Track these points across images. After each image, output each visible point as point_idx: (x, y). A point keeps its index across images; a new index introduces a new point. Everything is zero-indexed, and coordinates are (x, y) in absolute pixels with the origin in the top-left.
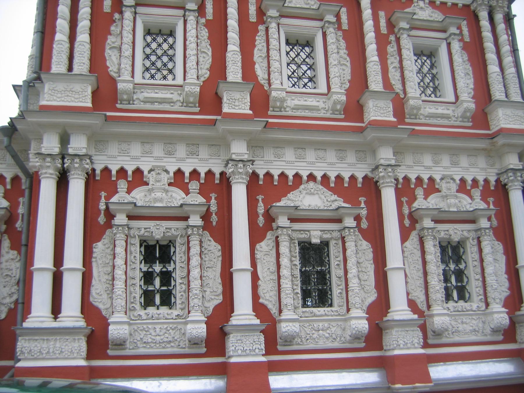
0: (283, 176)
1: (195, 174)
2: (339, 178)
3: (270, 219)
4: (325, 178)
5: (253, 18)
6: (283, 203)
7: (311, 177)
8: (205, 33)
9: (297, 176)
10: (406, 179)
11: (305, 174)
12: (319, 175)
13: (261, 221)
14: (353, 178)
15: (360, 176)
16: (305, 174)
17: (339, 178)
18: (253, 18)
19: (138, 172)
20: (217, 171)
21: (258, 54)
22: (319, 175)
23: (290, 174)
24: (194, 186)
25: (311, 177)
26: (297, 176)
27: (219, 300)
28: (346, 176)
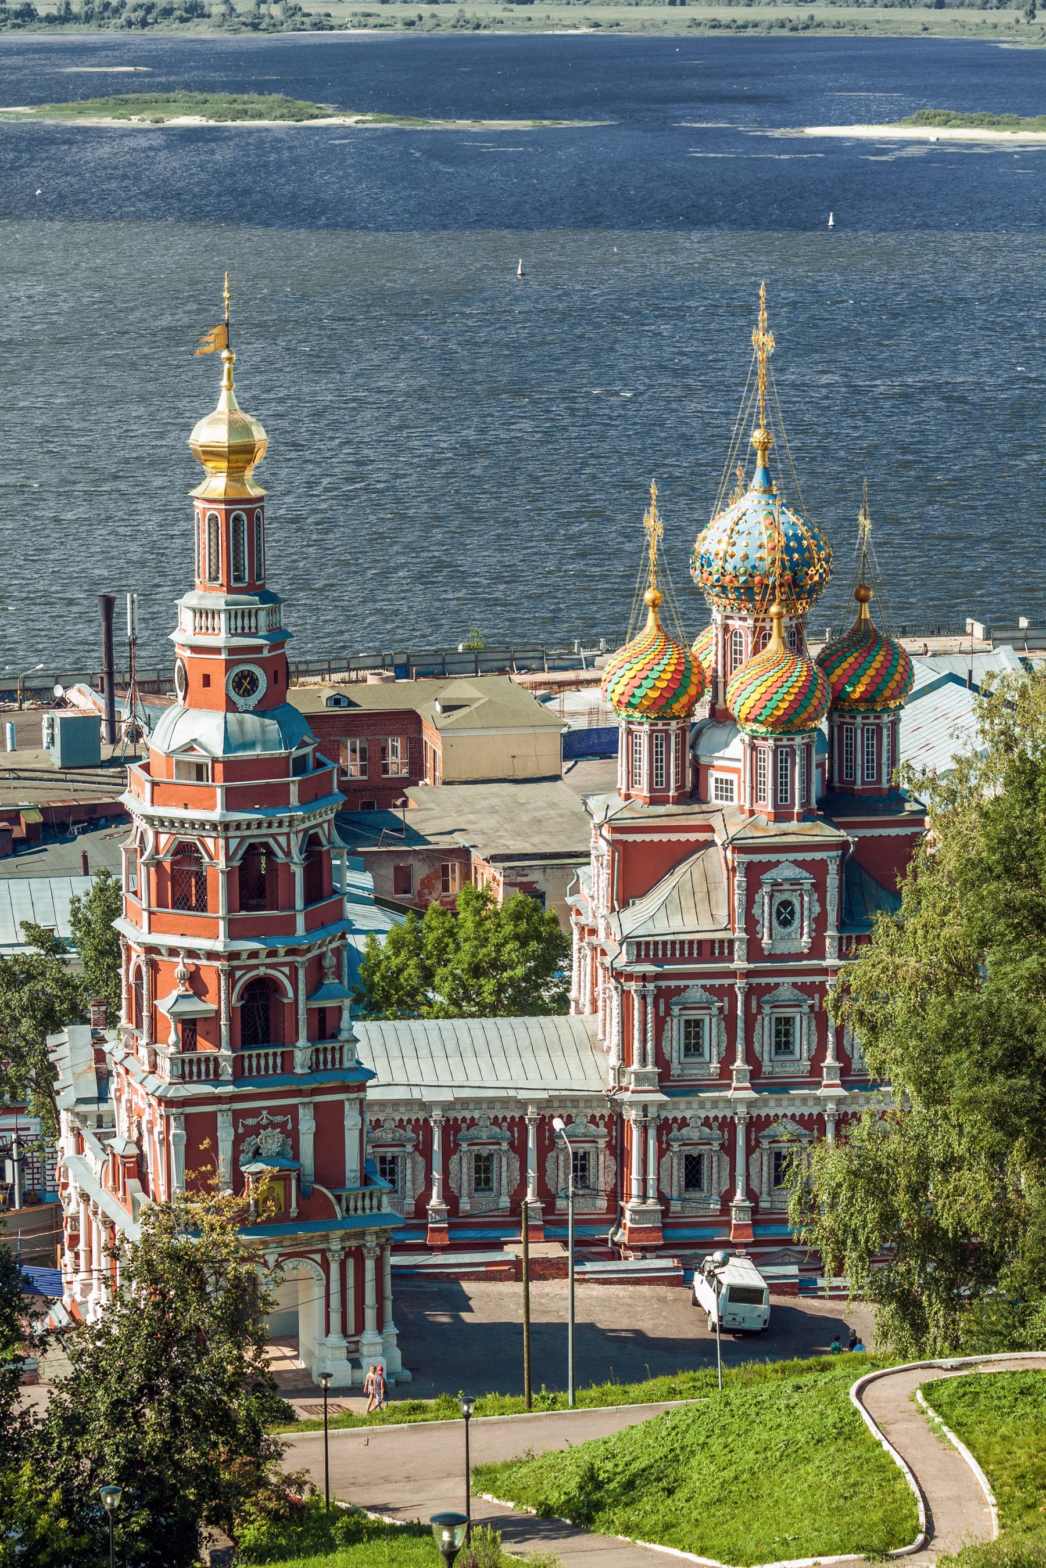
0: (768, 1116)
1: (716, 1118)
2: (802, 1115)
3: (758, 1142)
4: (793, 1116)
5: (754, 1011)
6: (765, 1133)
7: (785, 1116)
8: (723, 1024)
9: (776, 1115)
10: (846, 1114)
11: (780, 1114)
12: (789, 1114)
13: (753, 1143)
14: (811, 1115)
15: (815, 1113)
16: (780, 1114)
17: (802, 1115)
18: (754, 1011)
19: (684, 1118)
20: (729, 1115)
21: (756, 1037)
22: (789, 1114)
23: (772, 1115)
24: (715, 1124)
25: (785, 1116)
26: (776, 1115)
27: (727, 1187)
28: (806, 1114)
